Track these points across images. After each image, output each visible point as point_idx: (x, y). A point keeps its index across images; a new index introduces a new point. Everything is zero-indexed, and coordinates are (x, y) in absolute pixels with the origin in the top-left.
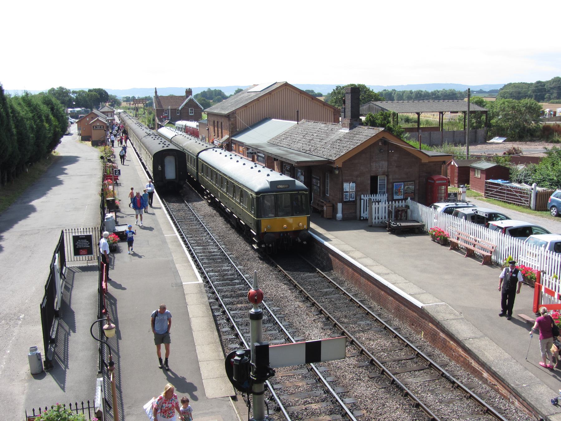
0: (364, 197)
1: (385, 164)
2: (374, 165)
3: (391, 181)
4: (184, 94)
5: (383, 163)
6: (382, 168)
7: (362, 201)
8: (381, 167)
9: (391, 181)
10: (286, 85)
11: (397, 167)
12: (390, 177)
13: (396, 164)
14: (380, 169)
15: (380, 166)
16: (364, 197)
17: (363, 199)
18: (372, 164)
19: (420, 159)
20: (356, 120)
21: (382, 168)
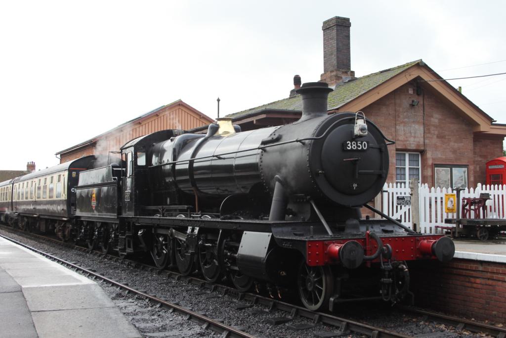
0: (389, 187)
1: (419, 129)
2: (400, 128)
3: (430, 162)
4: (25, 169)
5: (417, 126)
6: (415, 137)
7: (385, 194)
8: (413, 135)
9: (430, 162)
10: (179, 105)
11: (438, 137)
12: (429, 155)
13: (436, 132)
14: (412, 139)
15: (411, 133)
16: (389, 187)
17: (387, 191)
18: (397, 127)
19: (478, 125)
20: (346, 72)
21: (415, 137)
